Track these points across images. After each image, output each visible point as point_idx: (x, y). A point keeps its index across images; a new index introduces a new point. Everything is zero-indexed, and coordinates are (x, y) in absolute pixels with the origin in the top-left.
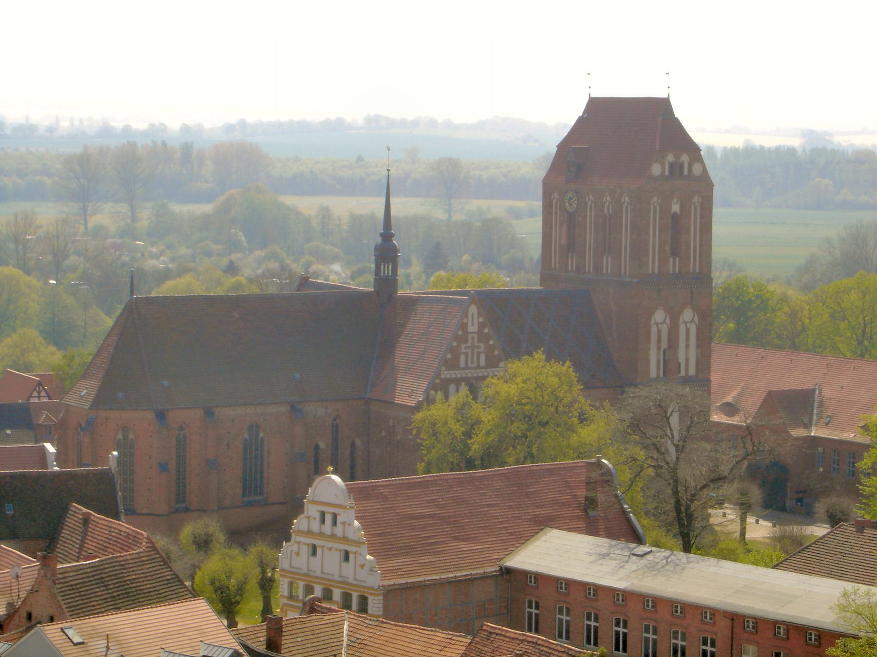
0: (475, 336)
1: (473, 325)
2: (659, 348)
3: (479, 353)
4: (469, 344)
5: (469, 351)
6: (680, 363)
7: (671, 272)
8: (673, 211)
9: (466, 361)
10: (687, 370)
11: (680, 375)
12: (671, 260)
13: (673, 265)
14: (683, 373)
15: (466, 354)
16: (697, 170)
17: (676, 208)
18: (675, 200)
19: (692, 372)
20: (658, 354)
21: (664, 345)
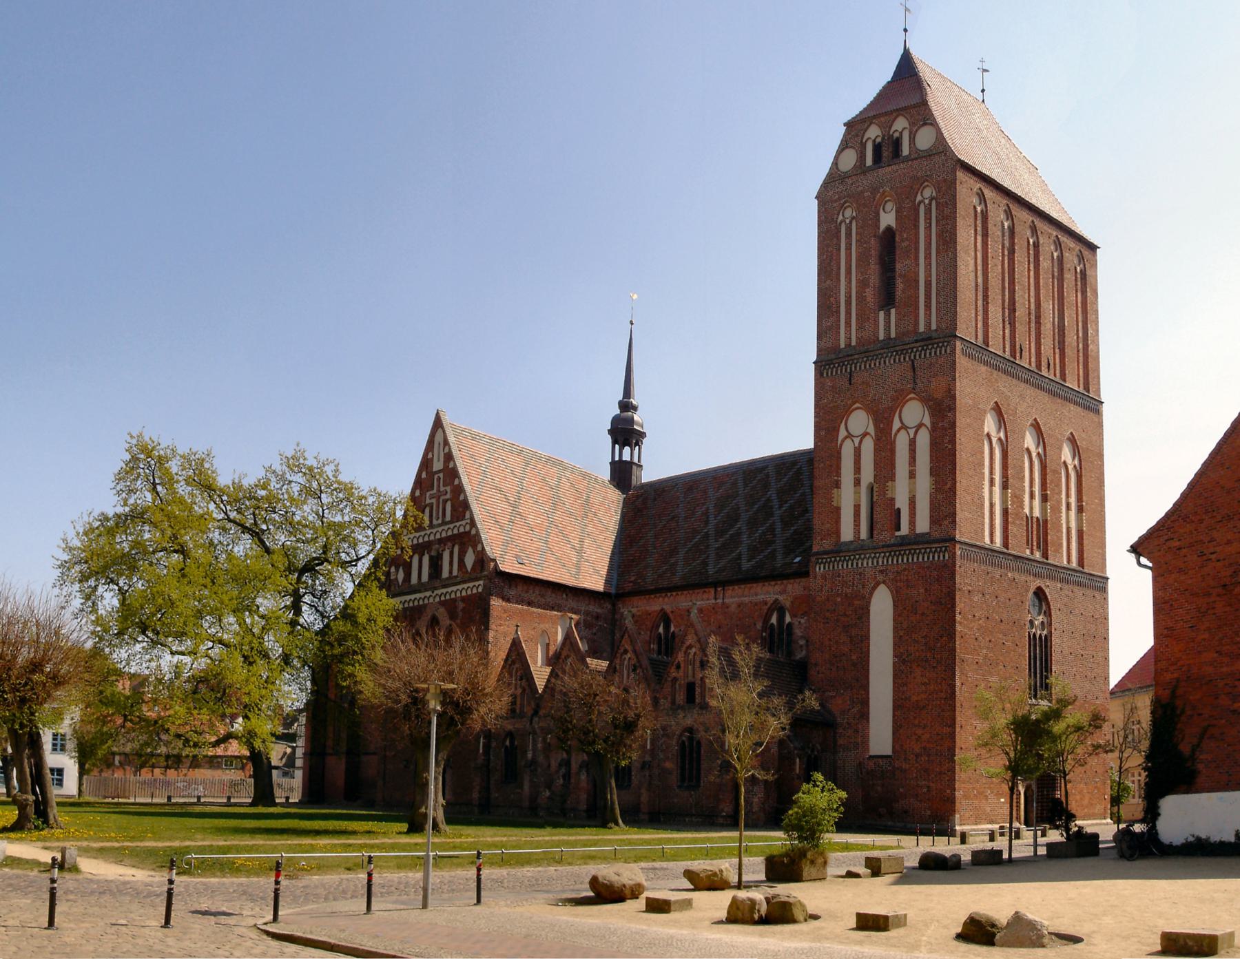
0: (441, 475)
1: (439, 460)
2: (857, 482)
3: (445, 501)
4: (435, 491)
5: (434, 501)
6: (899, 510)
7: (881, 337)
8: (883, 226)
9: (431, 516)
10: (912, 522)
11: (897, 534)
12: (882, 314)
13: (886, 325)
14: (905, 530)
15: (431, 506)
16: (925, 139)
17: (888, 219)
18: (889, 206)
19: (923, 526)
20: (857, 493)
21: (868, 475)
